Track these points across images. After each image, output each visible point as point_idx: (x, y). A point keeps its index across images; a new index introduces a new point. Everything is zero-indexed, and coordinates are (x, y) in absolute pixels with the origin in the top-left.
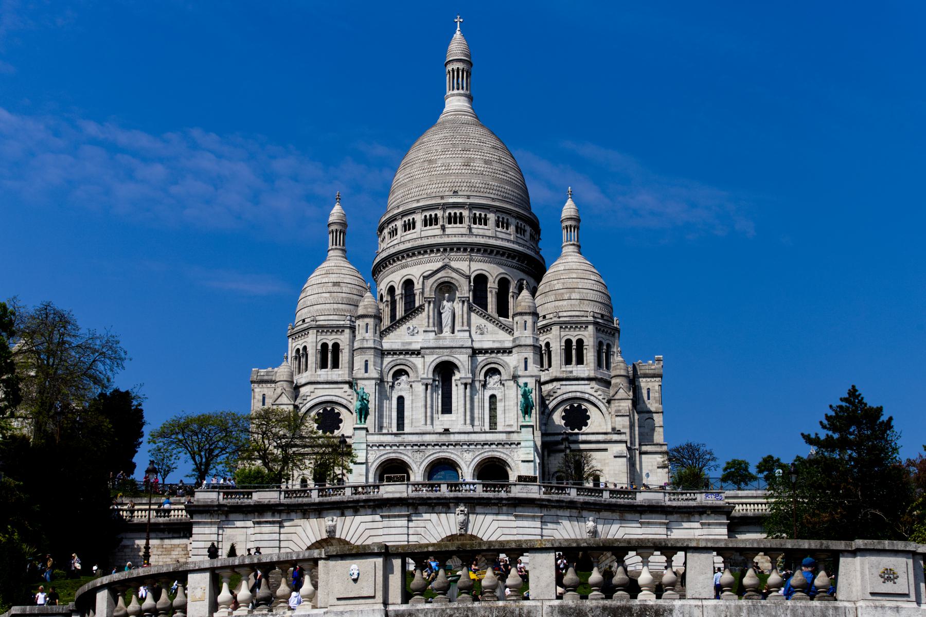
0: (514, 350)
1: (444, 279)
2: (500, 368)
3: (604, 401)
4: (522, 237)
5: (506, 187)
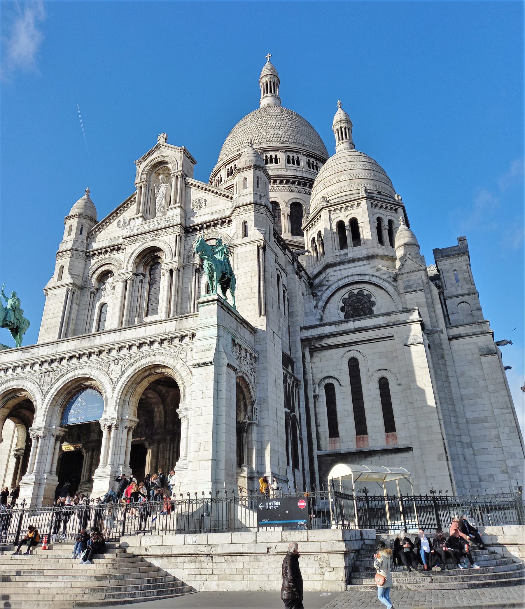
0: (233, 216)
3: (389, 280)
5: (297, 136)
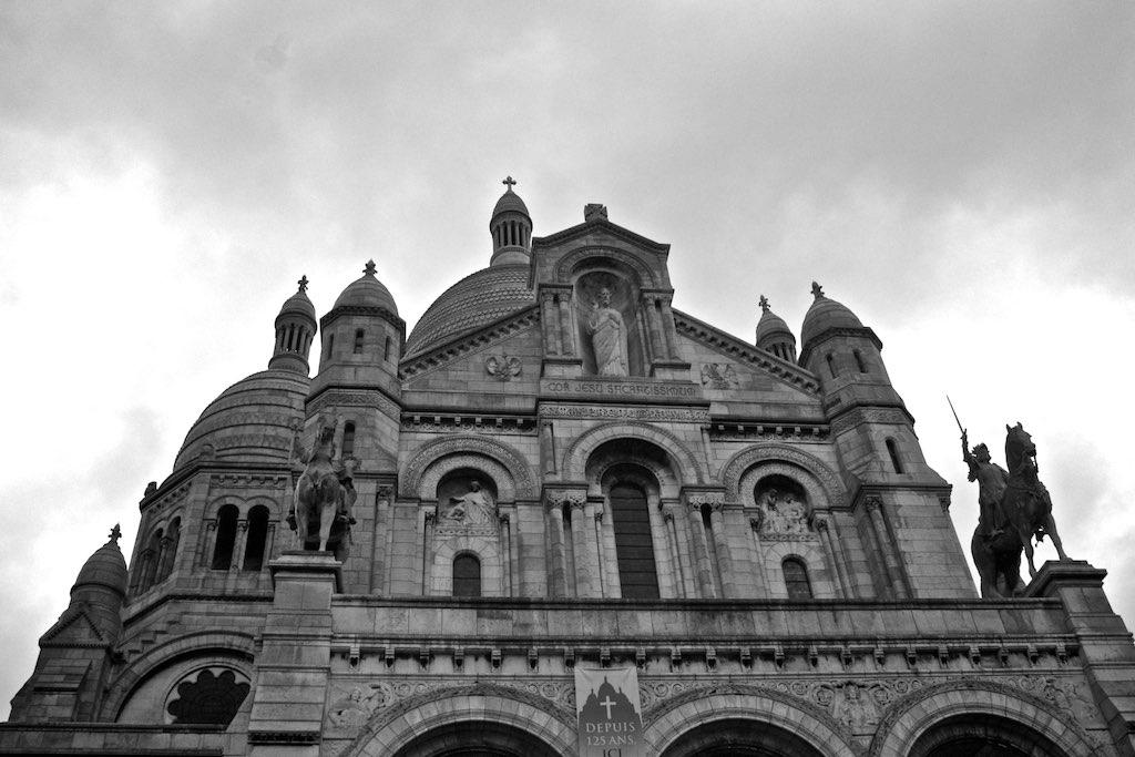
0: (834, 423)
2: (803, 479)
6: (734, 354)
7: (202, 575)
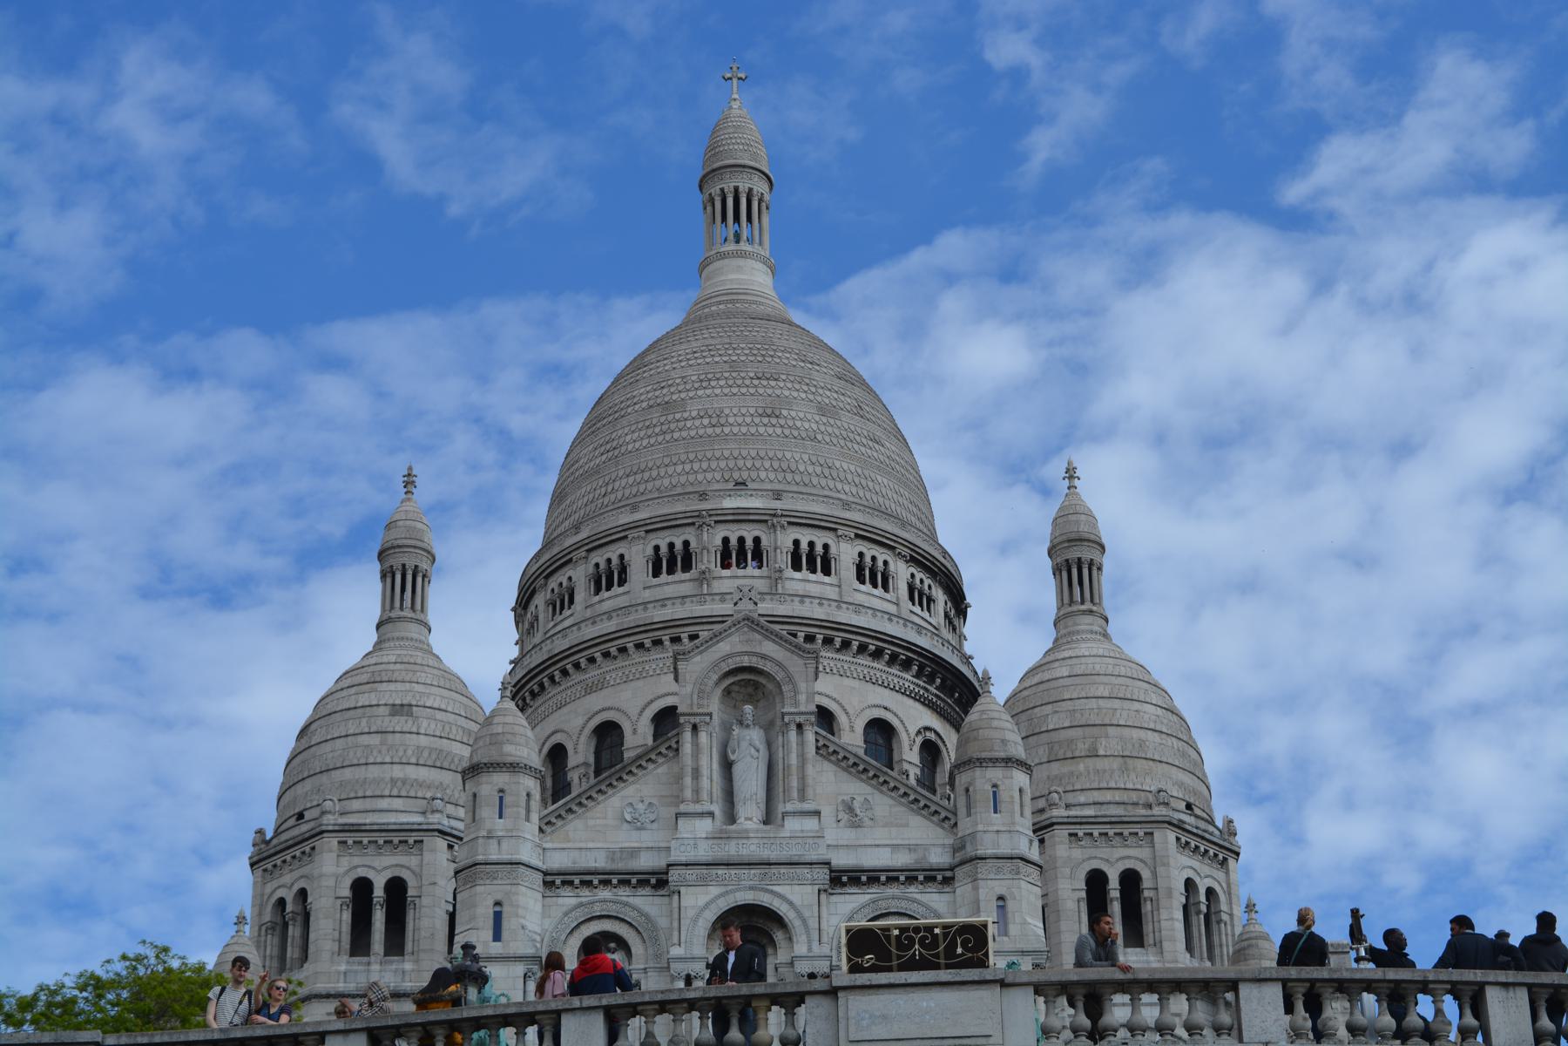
0: (959, 872)
1: (738, 658)
4: (926, 615)
5: (879, 478)
6: (874, 782)
7: (343, 968)
